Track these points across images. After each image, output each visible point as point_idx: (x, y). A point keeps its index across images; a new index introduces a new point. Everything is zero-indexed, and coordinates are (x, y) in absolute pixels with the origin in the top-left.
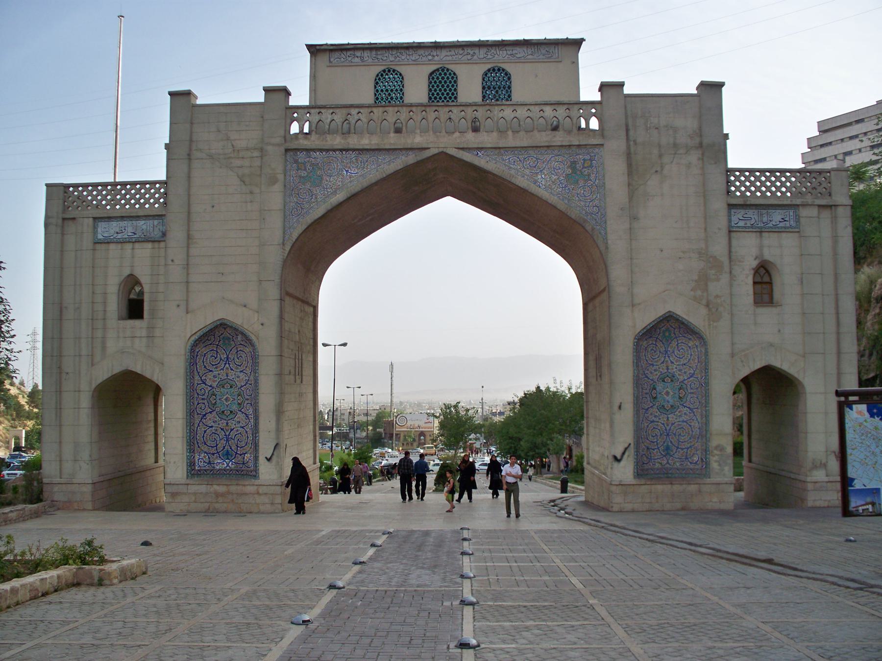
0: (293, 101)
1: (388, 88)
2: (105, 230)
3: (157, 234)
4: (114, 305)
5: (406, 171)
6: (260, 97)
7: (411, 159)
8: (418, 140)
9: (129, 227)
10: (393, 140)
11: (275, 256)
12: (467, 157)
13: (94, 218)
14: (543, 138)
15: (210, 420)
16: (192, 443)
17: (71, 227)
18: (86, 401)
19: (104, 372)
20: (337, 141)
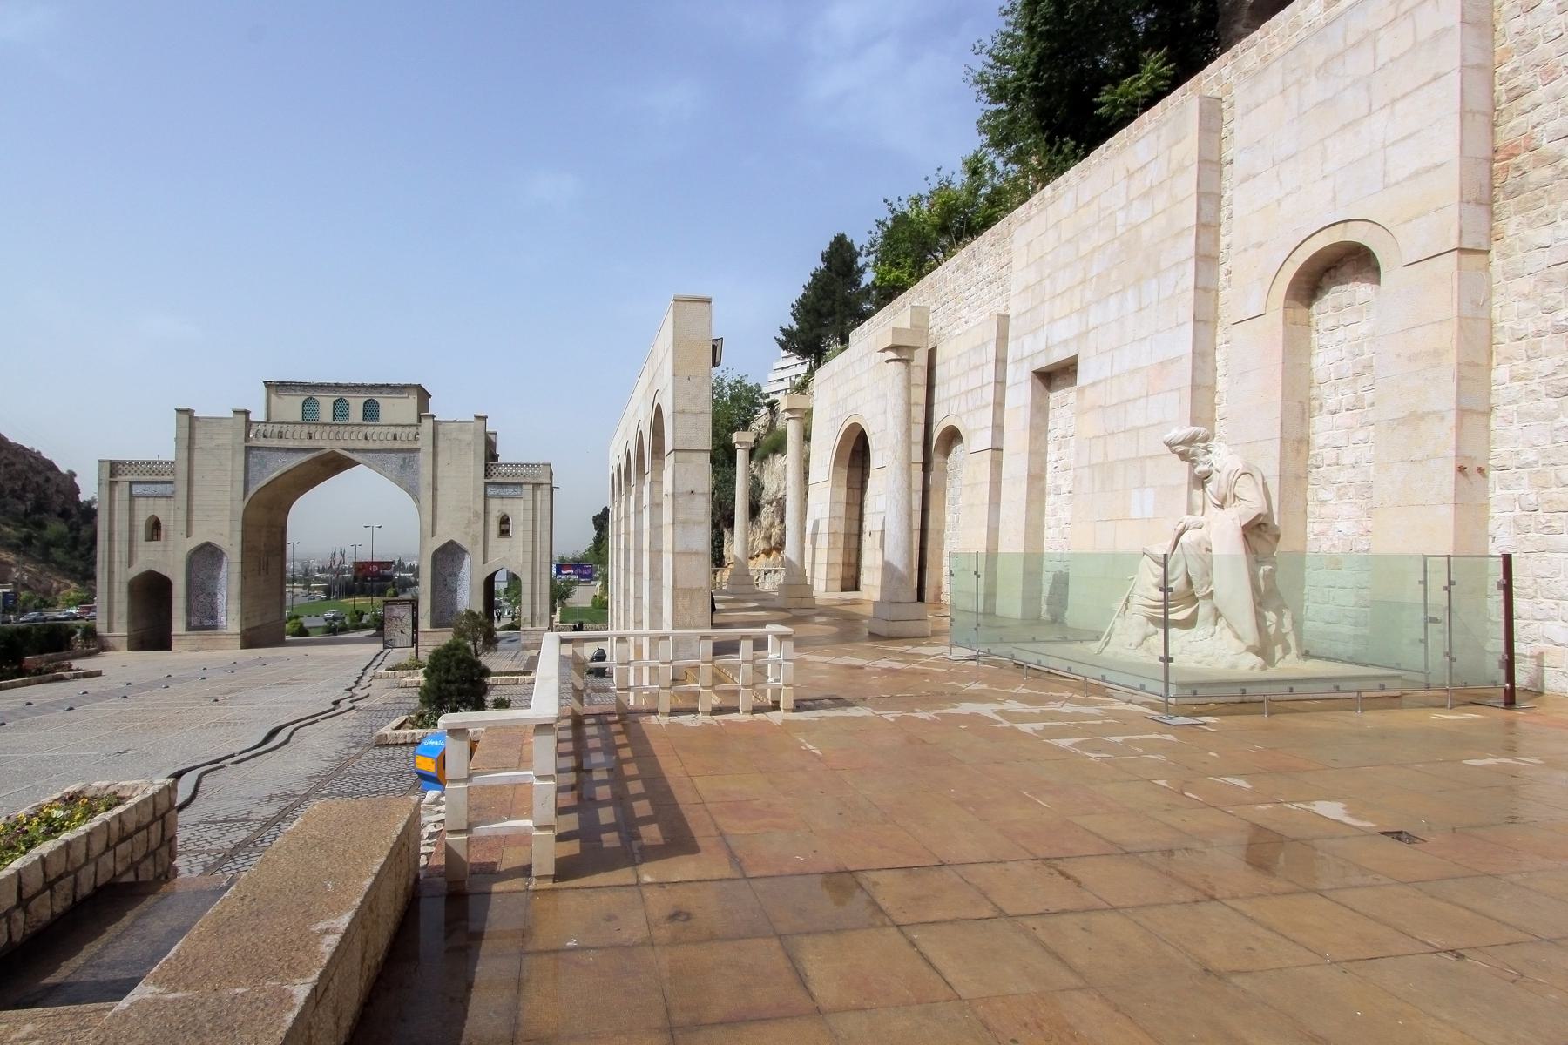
0: (252, 418)
1: (309, 407)
2: (137, 489)
3: (168, 492)
4: (141, 531)
5: (315, 459)
6: (231, 415)
7: (316, 454)
8: (321, 444)
9: (152, 489)
10: (307, 444)
11: (240, 507)
12: (346, 454)
13: (131, 483)
14: (389, 445)
15: (201, 598)
16: (189, 611)
17: (117, 488)
18: (125, 589)
19: (135, 571)
20: (275, 443)
